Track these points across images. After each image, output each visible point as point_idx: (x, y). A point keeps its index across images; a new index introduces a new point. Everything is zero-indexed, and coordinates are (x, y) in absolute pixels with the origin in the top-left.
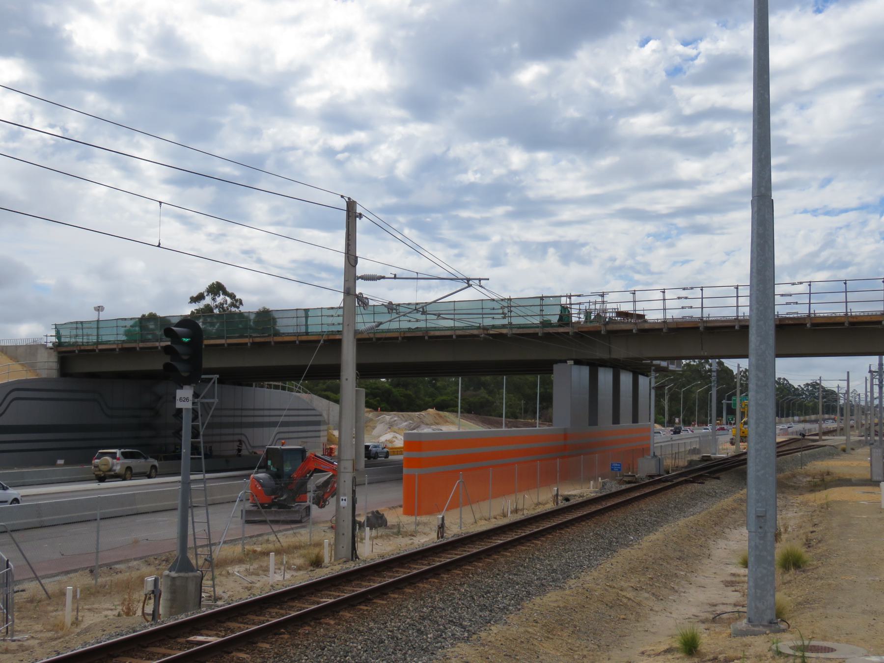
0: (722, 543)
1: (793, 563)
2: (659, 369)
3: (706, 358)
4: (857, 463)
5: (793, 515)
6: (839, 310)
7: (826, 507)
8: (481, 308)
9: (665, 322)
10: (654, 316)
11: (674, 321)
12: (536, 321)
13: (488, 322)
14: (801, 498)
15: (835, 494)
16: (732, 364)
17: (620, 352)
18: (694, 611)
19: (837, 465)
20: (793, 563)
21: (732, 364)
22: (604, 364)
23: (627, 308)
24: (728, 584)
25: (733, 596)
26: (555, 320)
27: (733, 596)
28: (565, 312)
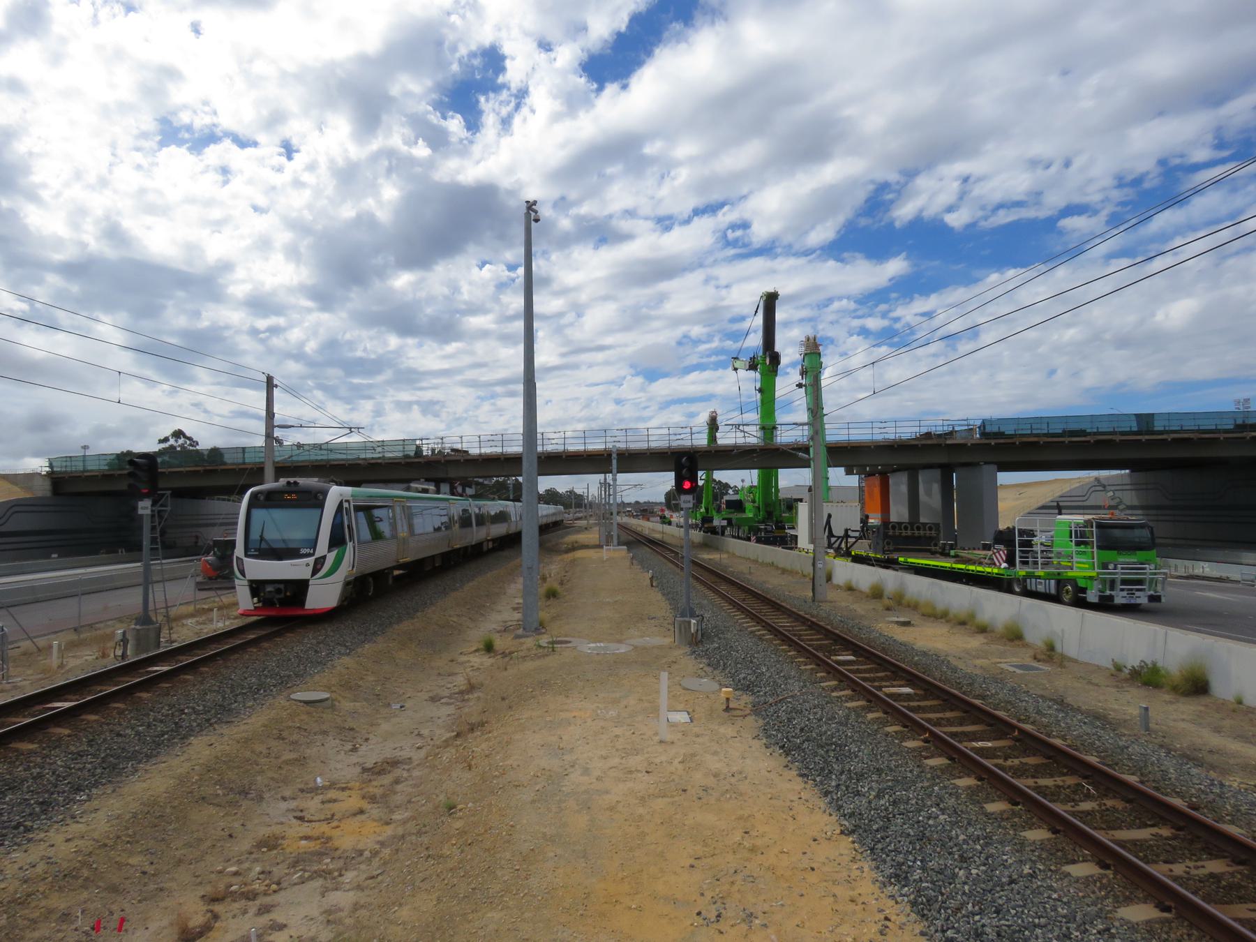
0: (513, 586)
1: (552, 594)
2: (477, 484)
3: (508, 476)
4: (592, 537)
5: (554, 567)
6: (581, 448)
7: (573, 561)
8: (365, 447)
9: (480, 455)
10: (474, 451)
11: (486, 454)
12: (400, 455)
13: (369, 456)
14: (560, 558)
15: (579, 554)
16: (520, 479)
17: (453, 473)
18: (494, 626)
19: (582, 538)
20: (552, 594)
21: (520, 479)
22: (444, 480)
23: (459, 446)
24: (514, 609)
25: (517, 616)
26: (412, 454)
27: (517, 616)
28: (419, 450)
